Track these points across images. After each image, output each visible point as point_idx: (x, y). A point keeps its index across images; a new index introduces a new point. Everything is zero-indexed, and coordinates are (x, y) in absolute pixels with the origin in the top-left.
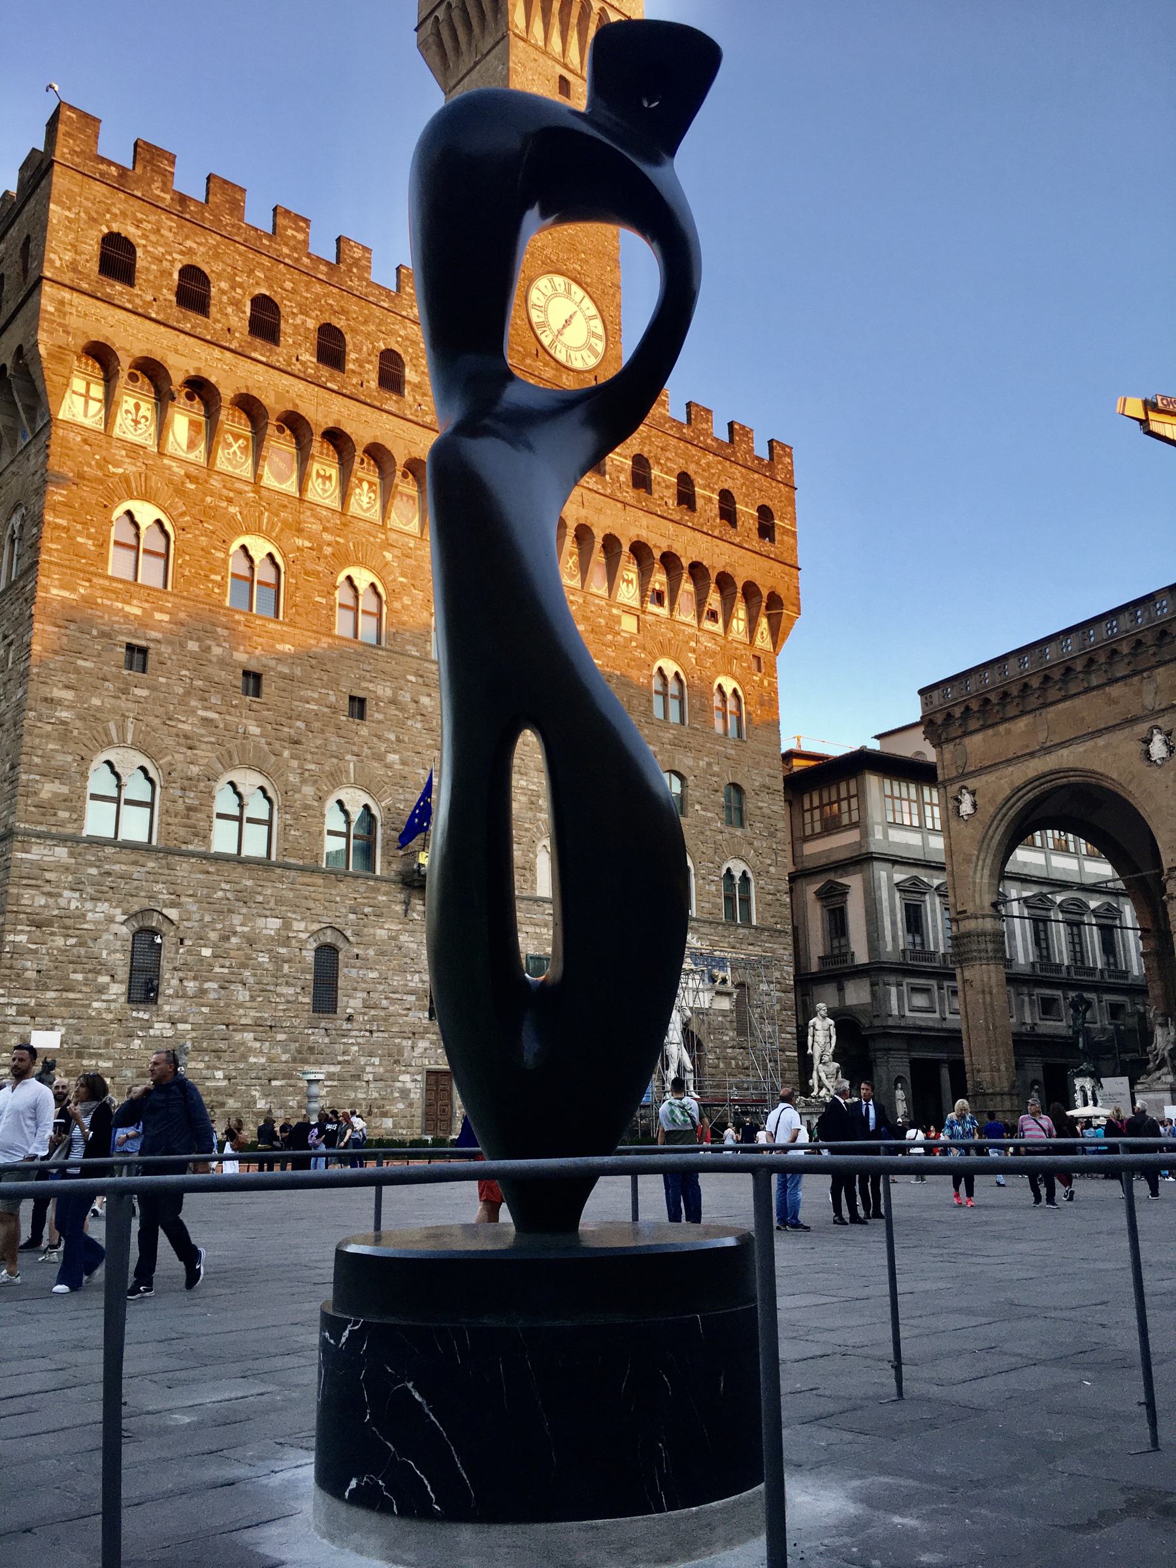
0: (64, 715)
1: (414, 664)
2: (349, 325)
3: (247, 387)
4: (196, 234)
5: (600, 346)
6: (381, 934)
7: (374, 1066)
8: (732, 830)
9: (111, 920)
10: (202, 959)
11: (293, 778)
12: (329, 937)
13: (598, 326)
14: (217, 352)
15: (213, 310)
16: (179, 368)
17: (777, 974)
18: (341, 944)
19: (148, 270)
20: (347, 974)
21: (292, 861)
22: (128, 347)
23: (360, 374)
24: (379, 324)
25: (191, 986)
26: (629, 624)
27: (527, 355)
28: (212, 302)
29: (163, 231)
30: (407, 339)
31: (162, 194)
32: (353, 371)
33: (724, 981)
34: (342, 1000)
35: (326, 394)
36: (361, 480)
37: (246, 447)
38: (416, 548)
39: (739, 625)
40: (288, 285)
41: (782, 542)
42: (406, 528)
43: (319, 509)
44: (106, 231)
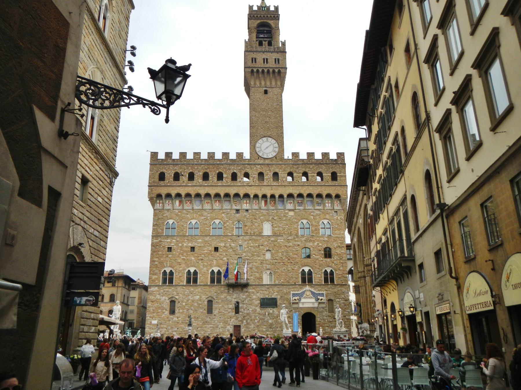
0: (156, 263)
1: (230, 237)
5: (277, 150)
6: (223, 297)
7: (221, 325)
8: (326, 259)
9: (165, 300)
10: (183, 305)
11: (201, 267)
12: (210, 299)
13: (276, 145)
14: (181, 187)
16: (173, 192)
17: (343, 296)
18: (213, 300)
20: (215, 306)
21: (202, 284)
25: (181, 311)
26: (291, 213)
27: (256, 159)
33: (322, 299)
34: (213, 311)
39: (328, 205)
40: (196, 168)
41: (340, 180)
42: (228, 208)
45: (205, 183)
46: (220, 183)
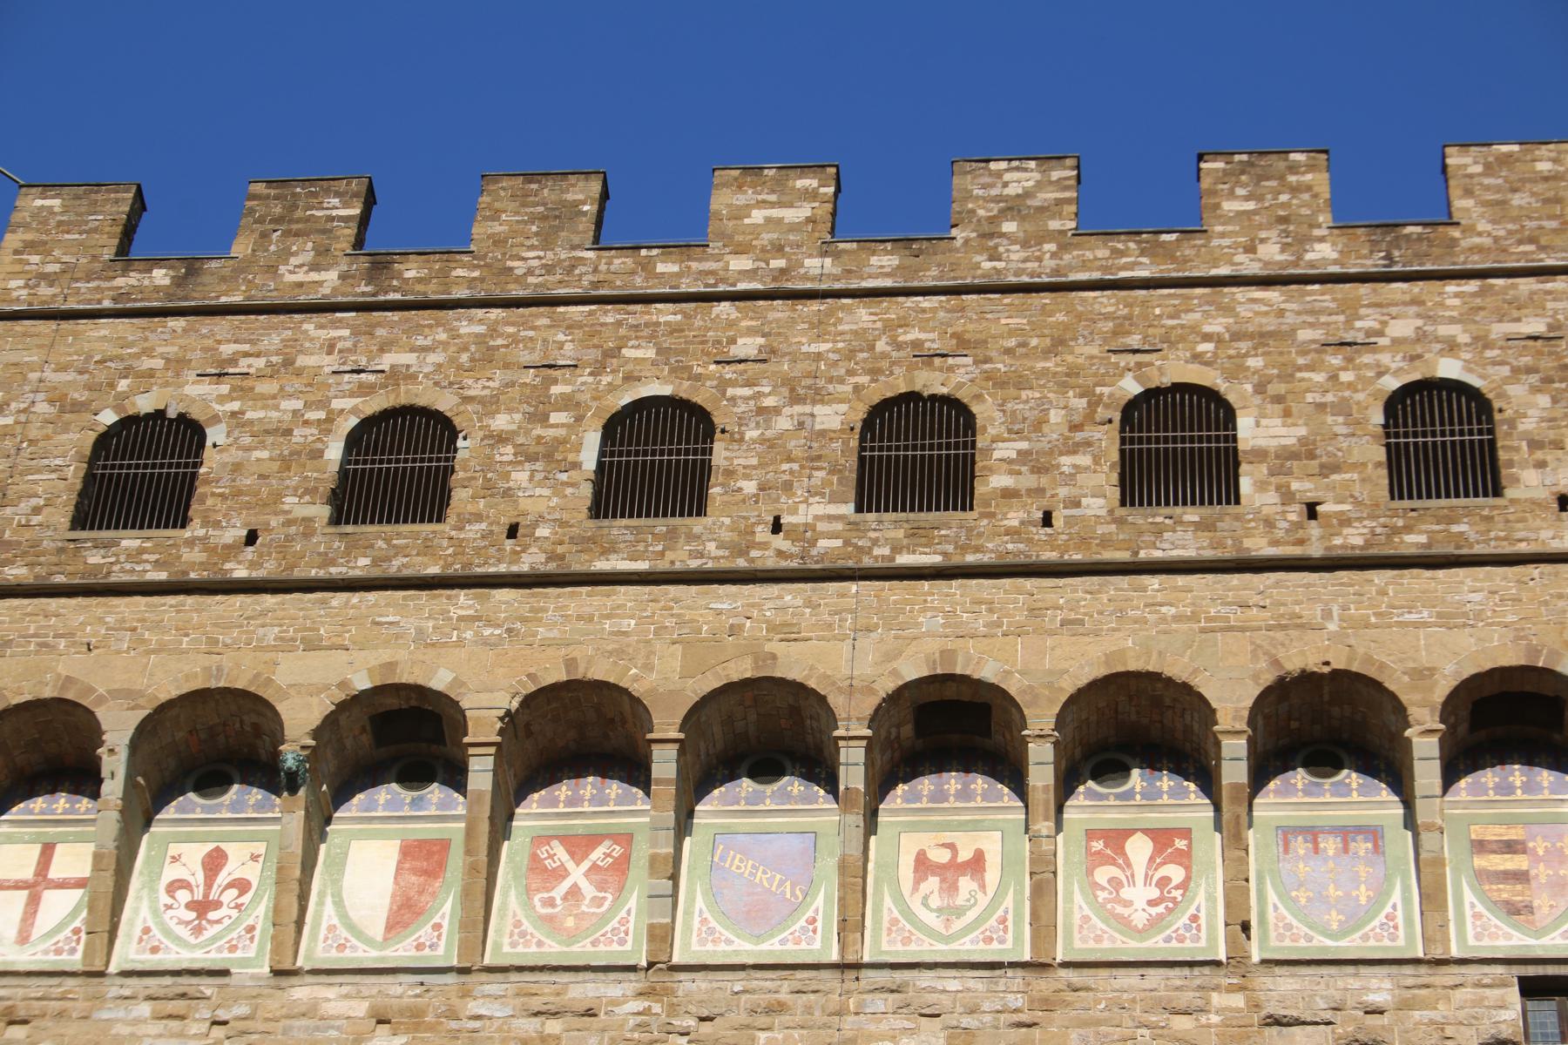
2: (988, 376)
3: (570, 663)
4: (418, 329)
15: (461, 497)
19: (237, 468)
22: (140, 683)
23: (1040, 491)
24: (1115, 333)
28: (460, 475)
29: (301, 361)
30: (1236, 337)
31: (314, 276)
32: (1008, 494)
35: (895, 591)
36: (1117, 838)
37: (621, 866)
38: (1405, 1005)
40: (747, 346)
43: (925, 979)
44: (109, 418)
45: (888, 536)
46: (1181, 531)
